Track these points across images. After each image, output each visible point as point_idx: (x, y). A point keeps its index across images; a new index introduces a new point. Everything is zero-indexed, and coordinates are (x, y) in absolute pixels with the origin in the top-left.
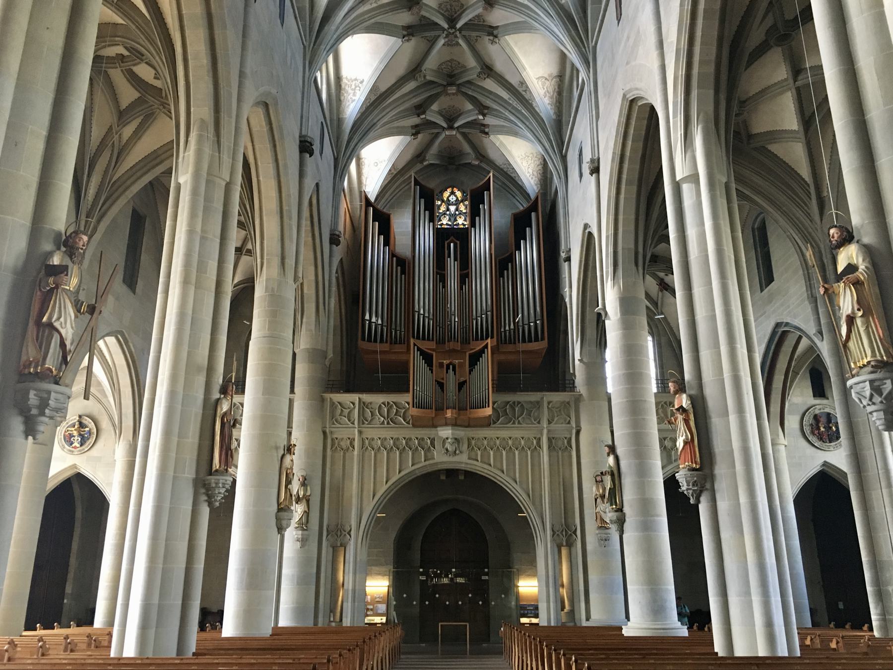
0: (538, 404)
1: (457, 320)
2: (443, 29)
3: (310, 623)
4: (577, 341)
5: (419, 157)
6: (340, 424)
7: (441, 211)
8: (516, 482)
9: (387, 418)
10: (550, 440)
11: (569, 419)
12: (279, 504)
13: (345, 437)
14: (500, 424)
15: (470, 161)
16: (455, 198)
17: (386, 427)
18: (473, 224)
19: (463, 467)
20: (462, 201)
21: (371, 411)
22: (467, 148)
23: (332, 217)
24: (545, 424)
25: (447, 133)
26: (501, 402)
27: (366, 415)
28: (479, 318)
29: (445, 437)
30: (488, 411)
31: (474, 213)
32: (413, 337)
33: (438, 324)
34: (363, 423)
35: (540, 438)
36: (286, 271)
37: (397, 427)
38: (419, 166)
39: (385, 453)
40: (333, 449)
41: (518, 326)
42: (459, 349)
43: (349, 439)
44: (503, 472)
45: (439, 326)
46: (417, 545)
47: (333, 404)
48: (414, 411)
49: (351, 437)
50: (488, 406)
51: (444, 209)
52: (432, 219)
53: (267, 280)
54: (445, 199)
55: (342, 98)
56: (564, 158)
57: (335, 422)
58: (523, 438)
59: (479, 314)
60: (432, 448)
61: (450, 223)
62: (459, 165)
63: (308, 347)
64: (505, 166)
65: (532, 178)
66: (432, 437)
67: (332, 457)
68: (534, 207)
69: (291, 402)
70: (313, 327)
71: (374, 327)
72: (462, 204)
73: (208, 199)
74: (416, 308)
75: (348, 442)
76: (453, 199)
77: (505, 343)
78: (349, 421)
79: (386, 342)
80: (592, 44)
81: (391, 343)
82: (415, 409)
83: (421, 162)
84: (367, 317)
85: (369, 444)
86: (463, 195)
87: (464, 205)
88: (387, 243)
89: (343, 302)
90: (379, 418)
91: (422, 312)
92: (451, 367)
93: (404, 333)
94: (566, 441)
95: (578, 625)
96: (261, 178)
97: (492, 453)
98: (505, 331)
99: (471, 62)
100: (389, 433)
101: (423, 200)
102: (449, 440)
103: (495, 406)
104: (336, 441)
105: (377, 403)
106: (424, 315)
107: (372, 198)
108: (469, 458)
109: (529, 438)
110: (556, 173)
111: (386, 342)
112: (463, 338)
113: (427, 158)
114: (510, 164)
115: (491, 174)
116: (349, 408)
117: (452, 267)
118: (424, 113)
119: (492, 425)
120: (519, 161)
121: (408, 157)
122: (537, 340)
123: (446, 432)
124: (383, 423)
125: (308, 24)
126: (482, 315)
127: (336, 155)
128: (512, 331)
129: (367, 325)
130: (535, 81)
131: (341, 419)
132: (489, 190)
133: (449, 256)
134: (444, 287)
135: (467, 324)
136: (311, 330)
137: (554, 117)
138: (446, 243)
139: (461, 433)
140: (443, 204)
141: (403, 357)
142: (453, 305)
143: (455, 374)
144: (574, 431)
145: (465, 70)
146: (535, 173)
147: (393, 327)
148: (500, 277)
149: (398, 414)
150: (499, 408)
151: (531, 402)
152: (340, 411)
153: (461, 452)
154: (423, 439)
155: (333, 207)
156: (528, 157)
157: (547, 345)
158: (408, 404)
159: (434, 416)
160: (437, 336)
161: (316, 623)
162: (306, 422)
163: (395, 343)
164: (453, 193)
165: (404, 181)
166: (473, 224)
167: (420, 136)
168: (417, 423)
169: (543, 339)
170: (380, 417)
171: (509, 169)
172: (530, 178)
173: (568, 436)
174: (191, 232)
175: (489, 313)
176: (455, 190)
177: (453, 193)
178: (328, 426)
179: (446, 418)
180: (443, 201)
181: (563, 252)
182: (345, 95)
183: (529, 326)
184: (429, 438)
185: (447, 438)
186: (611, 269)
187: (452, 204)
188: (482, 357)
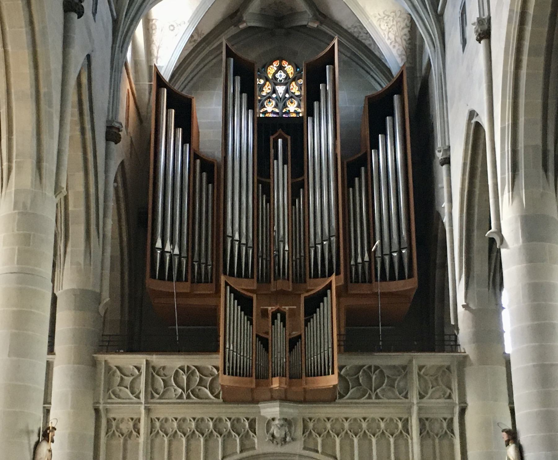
0: (405, 369)
1: (287, 248)
4: (460, 279)
6: (119, 397)
7: (264, 94)
9: (187, 391)
10: (422, 421)
11: (449, 391)
13: (127, 416)
14: (349, 398)
15: (304, 23)
16: (284, 75)
17: (184, 403)
18: (310, 112)
20: (294, 79)
21: (163, 380)
23: (109, 104)
26: (351, 368)
27: (157, 386)
28: (319, 246)
29: (269, 417)
30: (332, 380)
32: (225, 274)
33: (260, 254)
34: (153, 397)
35: (407, 420)
36: (44, 177)
37: (202, 403)
38: (233, 31)
39: (184, 440)
40: (110, 433)
41: (375, 257)
42: (290, 290)
43: (132, 419)
45: (262, 256)
47: (108, 369)
48: (225, 380)
49: (135, 417)
50: (333, 373)
51: (269, 91)
52: (251, 105)
53: (17, 192)
54: (270, 76)
56: (439, 18)
57: (113, 397)
58: (382, 419)
59: (319, 240)
60: (251, 434)
61: (277, 110)
62: (292, 28)
63: (75, 286)
64: (356, 30)
65: (394, 46)
66: (251, 417)
67: (108, 445)
69: (49, 366)
70: (81, 260)
71: (168, 258)
72: (294, 83)
74: (229, 232)
75: (131, 424)
77: (357, 282)
78: (132, 393)
79: (186, 280)
81: (193, 282)
82: (226, 376)
83: (236, 25)
84: (159, 244)
86: (295, 71)
87: (297, 84)
88: (187, 139)
89: (124, 223)
90: (175, 390)
91: (237, 237)
92: (279, 315)
93: (212, 269)
94: (445, 424)
96: (9, 48)
97: (338, 440)
98: (356, 264)
101: (239, 77)
102: (277, 422)
103: (342, 373)
104: (114, 423)
105: (172, 368)
106: (240, 241)
107: (166, 77)
108: (305, 448)
110: (429, 39)
111: (186, 280)
112: (296, 274)
113: (244, 19)
114: (362, 27)
115: (336, 42)
116: (132, 375)
119: (337, 401)
120: (375, 22)
122: (402, 277)
124: (181, 397)
126: (323, 241)
127: (115, 14)
128: (367, 264)
129: (159, 254)
131: (120, 390)
132: (333, 63)
133: (276, 158)
134: (268, 201)
135: (302, 254)
136: (78, 264)
139: (292, 411)
140: (268, 83)
141: (210, 302)
143: (284, 326)
144: (457, 410)
146: (399, 40)
147: (196, 258)
148: (348, 188)
149: (203, 384)
150: (348, 375)
151: (394, 367)
152: (119, 379)
153: (293, 439)
154: (238, 420)
155: (110, 88)
156: (389, 16)
157: (416, 285)
158: (217, 368)
159: (254, 386)
160: (258, 272)
162: (70, 397)
163: (199, 281)
164: (281, 68)
165: (211, 53)
166: (310, 112)
169: (411, 276)
170: (176, 387)
171: (362, 34)
172: (391, 47)
173: (449, 416)
175: (333, 239)
176: (285, 64)
177: (281, 68)
178: (101, 401)
179: (271, 390)
180: (267, 79)
181: (440, 151)
183: (391, 258)
184: (248, 419)
185: (273, 419)
186: (508, 175)
187: (281, 84)
188: (323, 302)
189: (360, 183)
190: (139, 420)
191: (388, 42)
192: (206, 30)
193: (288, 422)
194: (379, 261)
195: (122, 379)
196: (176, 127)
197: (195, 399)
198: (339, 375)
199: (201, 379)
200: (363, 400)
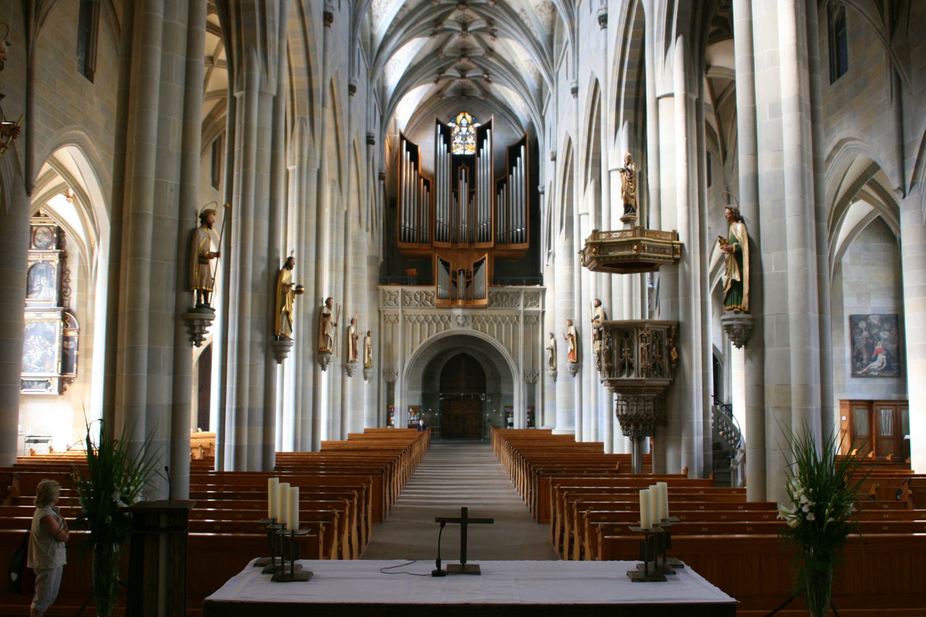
0: (518, 294)
2: (459, 32)
3: (375, 426)
5: (439, 93)
6: (389, 305)
7: (455, 132)
8: (502, 343)
10: (525, 317)
12: (364, 364)
16: (466, 122)
19: (469, 333)
22: (474, 87)
24: (521, 308)
25: (461, 80)
29: (457, 314)
30: (485, 302)
31: (480, 145)
32: (436, 240)
44: (494, 337)
46: (438, 377)
47: (384, 292)
49: (397, 314)
54: (459, 122)
55: (385, 72)
56: (543, 118)
61: (462, 142)
67: (385, 327)
68: (523, 142)
73: (338, 223)
74: (438, 219)
75: (395, 317)
76: (464, 122)
77: (500, 243)
78: (395, 303)
79: (417, 242)
80: (556, 71)
81: (420, 242)
84: (403, 221)
85: (409, 318)
88: (416, 168)
92: (462, 272)
94: (535, 318)
95: (537, 428)
97: (487, 325)
99: (476, 44)
100: (422, 312)
102: (460, 317)
104: (387, 317)
106: (443, 223)
108: (473, 328)
109: (512, 316)
117: (463, 187)
118: (443, 72)
121: (431, 93)
122: (522, 242)
123: (458, 312)
124: (417, 305)
125: (369, 52)
130: (524, 63)
132: (490, 128)
133: (461, 179)
134: (457, 201)
137: (537, 87)
138: (459, 168)
139: (467, 312)
141: (428, 253)
142: (464, 215)
145: (473, 48)
147: (421, 231)
153: (468, 324)
154: (443, 316)
158: (434, 292)
161: (378, 426)
163: (423, 242)
164: (464, 117)
167: (440, 82)
168: (438, 307)
169: (526, 242)
174: (331, 243)
175: (489, 223)
177: (464, 117)
178: (381, 307)
180: (457, 124)
182: (388, 69)
189: (503, 192)
190: (398, 315)
191: (521, 109)
192: (425, 100)
193: (465, 317)
194: (511, 233)
195: (390, 297)
196: (411, 160)
197: (424, 307)
198: (489, 295)
199: (426, 298)
200: (499, 307)
